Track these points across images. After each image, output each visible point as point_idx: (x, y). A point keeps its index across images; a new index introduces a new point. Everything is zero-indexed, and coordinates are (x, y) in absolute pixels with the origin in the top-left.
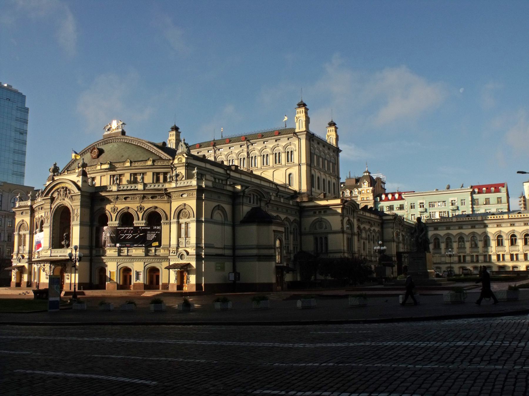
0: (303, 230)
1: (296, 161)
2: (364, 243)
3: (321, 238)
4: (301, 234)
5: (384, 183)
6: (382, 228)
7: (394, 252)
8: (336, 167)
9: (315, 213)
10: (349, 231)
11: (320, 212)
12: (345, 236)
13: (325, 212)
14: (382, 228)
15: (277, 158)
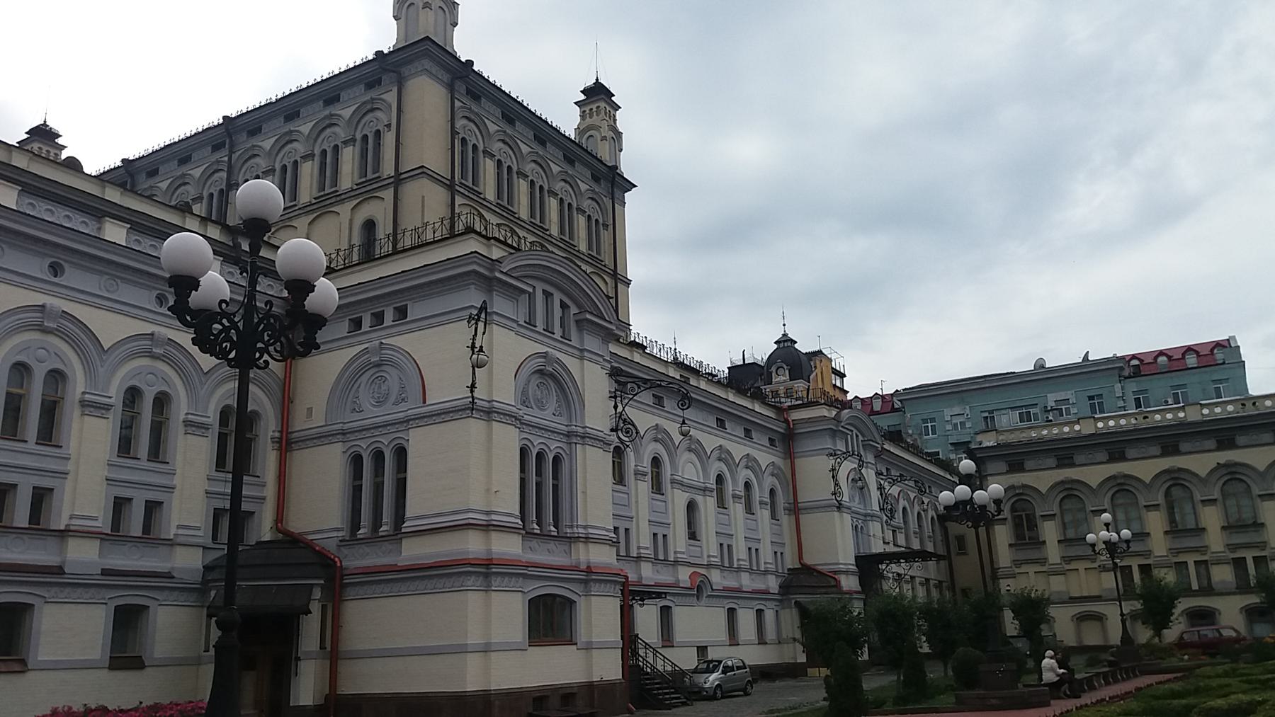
0: (300, 423)
1: (388, 169)
2: (691, 507)
3: (378, 456)
4: (286, 444)
5: (842, 376)
6: (790, 455)
7: (846, 557)
8: (606, 236)
9: (357, 324)
10: (547, 415)
11: (379, 318)
12: (508, 439)
13: (402, 313)
14: (790, 455)
15: (328, 163)
